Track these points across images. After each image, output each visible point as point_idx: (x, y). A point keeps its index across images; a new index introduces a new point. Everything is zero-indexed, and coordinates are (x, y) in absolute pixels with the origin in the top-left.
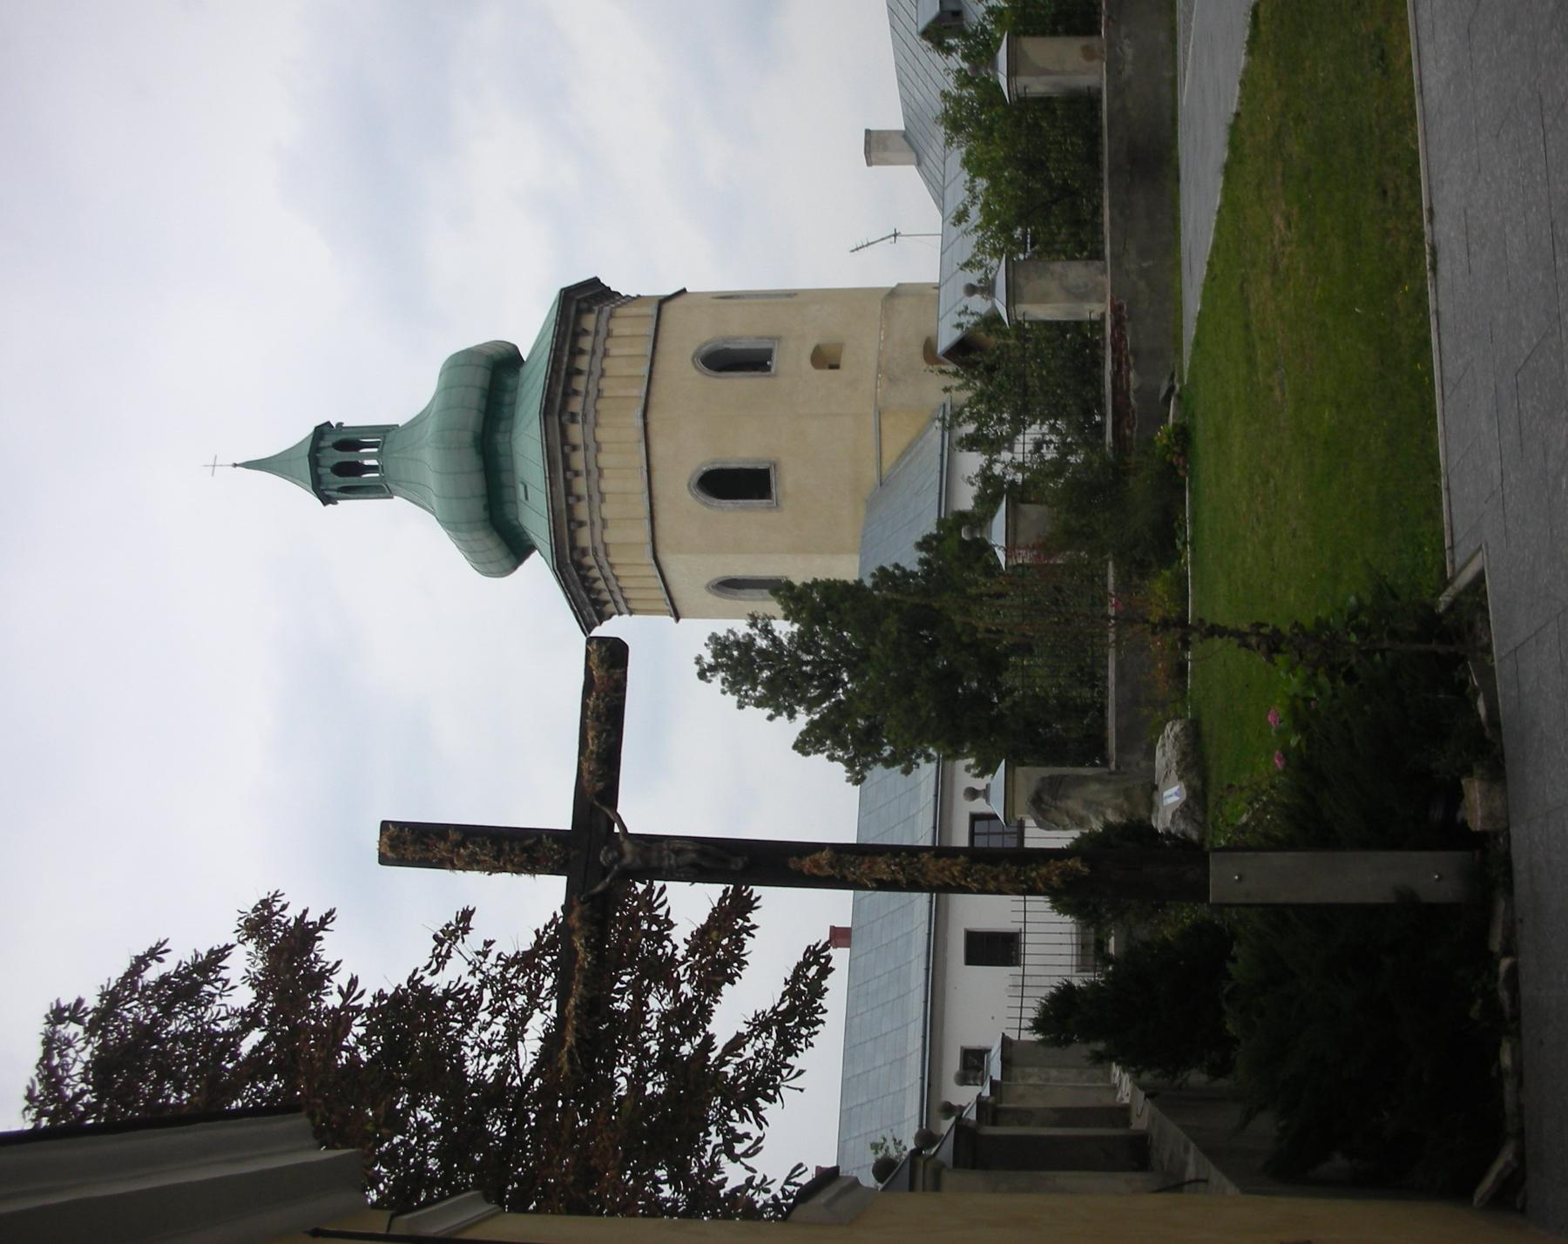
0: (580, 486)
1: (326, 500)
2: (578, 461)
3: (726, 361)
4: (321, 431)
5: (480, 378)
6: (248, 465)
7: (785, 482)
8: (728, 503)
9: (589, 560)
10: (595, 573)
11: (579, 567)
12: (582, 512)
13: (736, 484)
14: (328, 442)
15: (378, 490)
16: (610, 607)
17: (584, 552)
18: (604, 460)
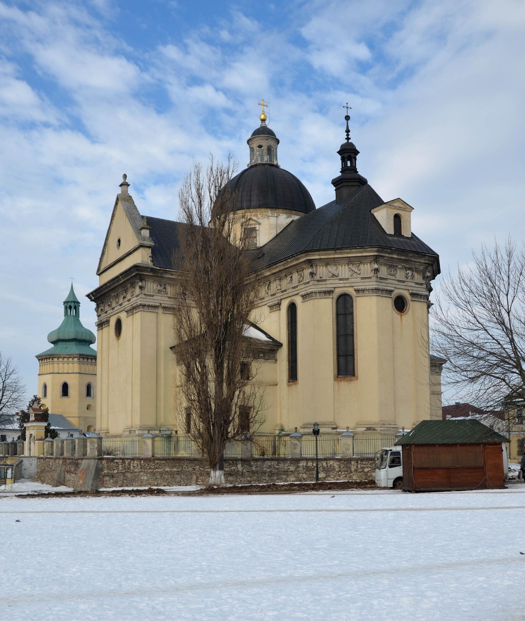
0: (66, 360)
1: (64, 303)
2: (70, 359)
3: (89, 388)
4: (78, 303)
5: (88, 338)
6: (72, 286)
7: (65, 399)
8: (61, 388)
9: (51, 360)
10: (48, 360)
11: (49, 358)
12: (61, 360)
13: (65, 390)
14: (76, 304)
15: (66, 314)
16: (41, 362)
17: (52, 359)
18: (71, 365)
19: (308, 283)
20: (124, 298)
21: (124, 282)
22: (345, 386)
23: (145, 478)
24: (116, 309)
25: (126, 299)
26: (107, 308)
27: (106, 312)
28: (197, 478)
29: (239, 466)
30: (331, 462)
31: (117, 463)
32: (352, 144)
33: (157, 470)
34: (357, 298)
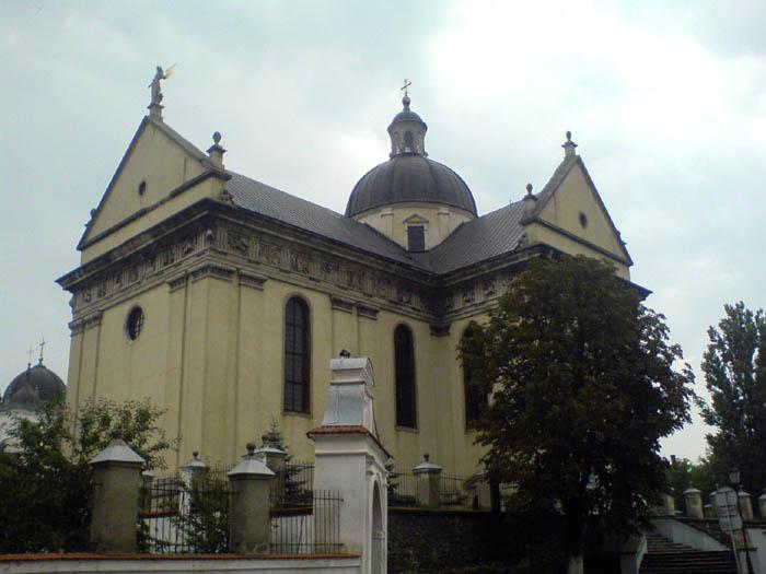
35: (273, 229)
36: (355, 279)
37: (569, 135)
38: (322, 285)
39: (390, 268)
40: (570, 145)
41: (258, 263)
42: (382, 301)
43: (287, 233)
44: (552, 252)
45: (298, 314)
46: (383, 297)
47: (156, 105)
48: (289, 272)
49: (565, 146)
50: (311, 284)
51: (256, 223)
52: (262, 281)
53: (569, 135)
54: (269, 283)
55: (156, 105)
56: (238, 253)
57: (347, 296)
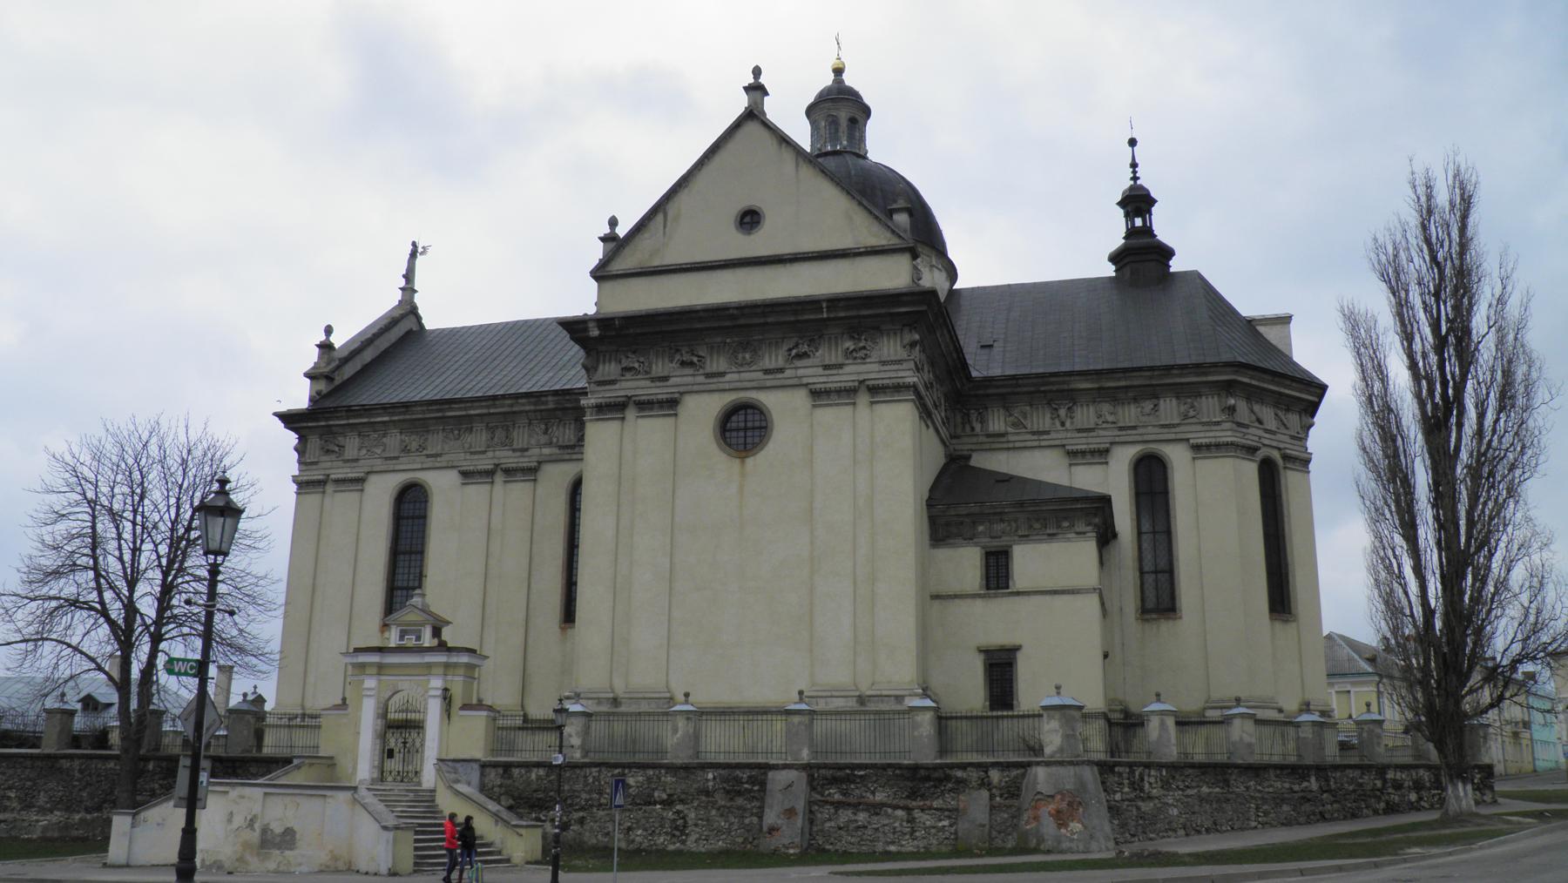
19: (1218, 423)
20: (804, 355)
21: (828, 319)
22: (1286, 632)
23: (1175, 812)
24: (728, 377)
25: (798, 363)
26: (659, 368)
27: (666, 379)
28: (1257, 808)
29: (1313, 779)
30: (1421, 772)
31: (1120, 774)
32: (1142, 188)
33: (1189, 792)
34: (1290, 474)
35: (361, 416)
36: (500, 434)
37: (757, 72)
38: (442, 461)
39: (546, 403)
40: (756, 90)
41: (357, 460)
42: (546, 451)
43: (379, 415)
44: (591, 325)
45: (410, 509)
46: (550, 444)
47: (409, 289)
48: (396, 458)
49: (748, 89)
50: (429, 463)
51: (338, 418)
52: (360, 481)
53: (757, 72)
54: (373, 479)
55: (409, 289)
56: (333, 457)
57: (485, 463)
